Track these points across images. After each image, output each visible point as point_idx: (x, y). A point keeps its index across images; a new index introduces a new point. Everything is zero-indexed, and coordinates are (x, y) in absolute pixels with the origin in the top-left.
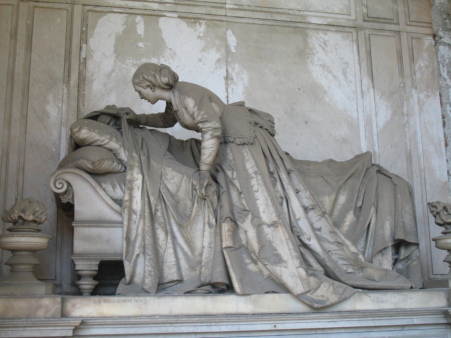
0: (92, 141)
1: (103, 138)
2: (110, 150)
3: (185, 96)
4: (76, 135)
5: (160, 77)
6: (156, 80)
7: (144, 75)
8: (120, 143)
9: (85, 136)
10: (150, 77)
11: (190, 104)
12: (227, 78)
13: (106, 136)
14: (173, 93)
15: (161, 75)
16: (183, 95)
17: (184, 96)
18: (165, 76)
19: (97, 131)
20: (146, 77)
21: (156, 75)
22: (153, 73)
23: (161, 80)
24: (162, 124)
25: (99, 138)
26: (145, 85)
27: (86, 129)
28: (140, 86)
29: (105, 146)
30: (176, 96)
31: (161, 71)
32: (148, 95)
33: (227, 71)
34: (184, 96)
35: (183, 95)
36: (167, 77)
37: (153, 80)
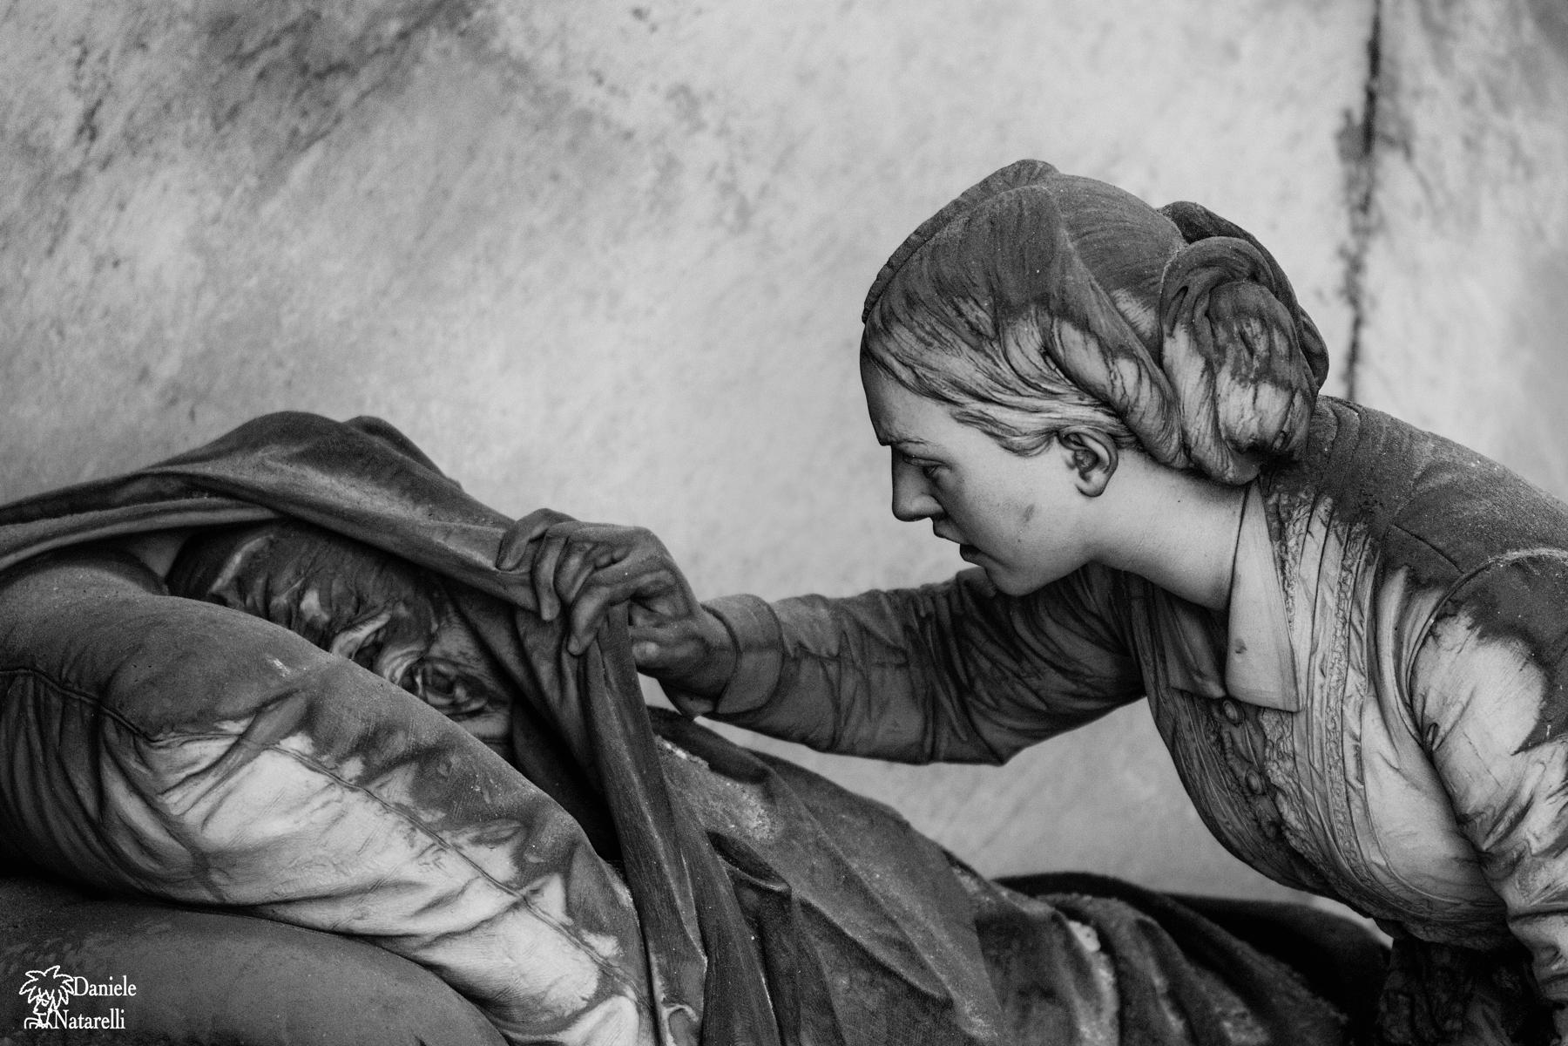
0: (325, 881)
1: (448, 872)
2: (487, 1002)
3: (1442, 615)
4: (175, 802)
5: (1211, 370)
6: (1170, 402)
7: (1070, 335)
8: (607, 946)
9: (275, 827)
10: (1127, 369)
11: (1485, 706)
12: (1366, 137)
13: (482, 853)
14: (1279, 534)
15: (1221, 350)
16: (1416, 585)
17: (1426, 605)
18: (1266, 373)
19: (397, 786)
20: (1090, 364)
21: (1178, 348)
22: (1146, 320)
23: (1214, 400)
24: (907, 724)
25: (412, 872)
26: (1035, 422)
27: (300, 758)
28: (966, 419)
29: (439, 956)
30: (1307, 568)
31: (1225, 304)
32: (1028, 513)
33: (1374, 52)
34: (1426, 605)
35: (1416, 585)
36: (1276, 382)
37: (1146, 401)
